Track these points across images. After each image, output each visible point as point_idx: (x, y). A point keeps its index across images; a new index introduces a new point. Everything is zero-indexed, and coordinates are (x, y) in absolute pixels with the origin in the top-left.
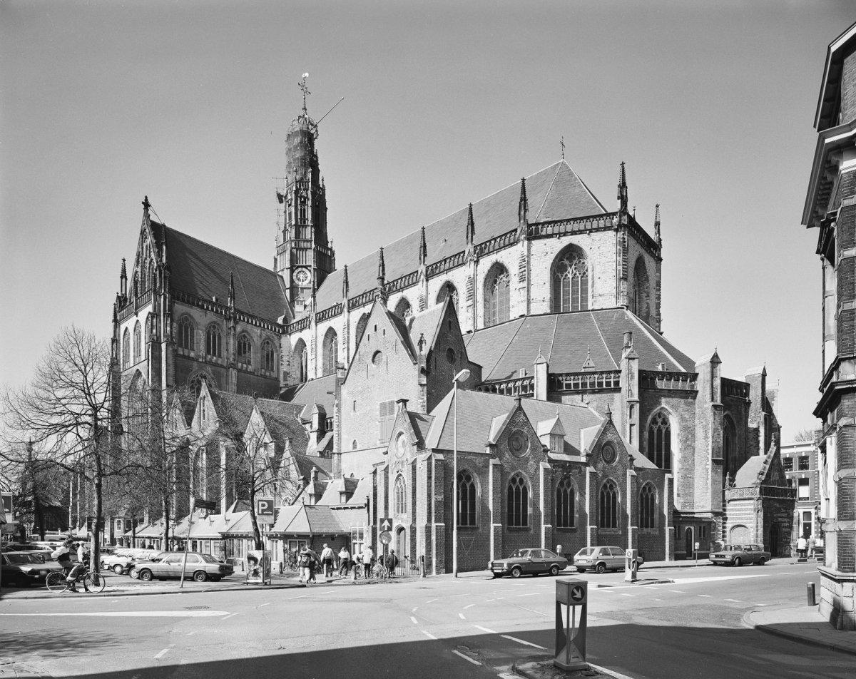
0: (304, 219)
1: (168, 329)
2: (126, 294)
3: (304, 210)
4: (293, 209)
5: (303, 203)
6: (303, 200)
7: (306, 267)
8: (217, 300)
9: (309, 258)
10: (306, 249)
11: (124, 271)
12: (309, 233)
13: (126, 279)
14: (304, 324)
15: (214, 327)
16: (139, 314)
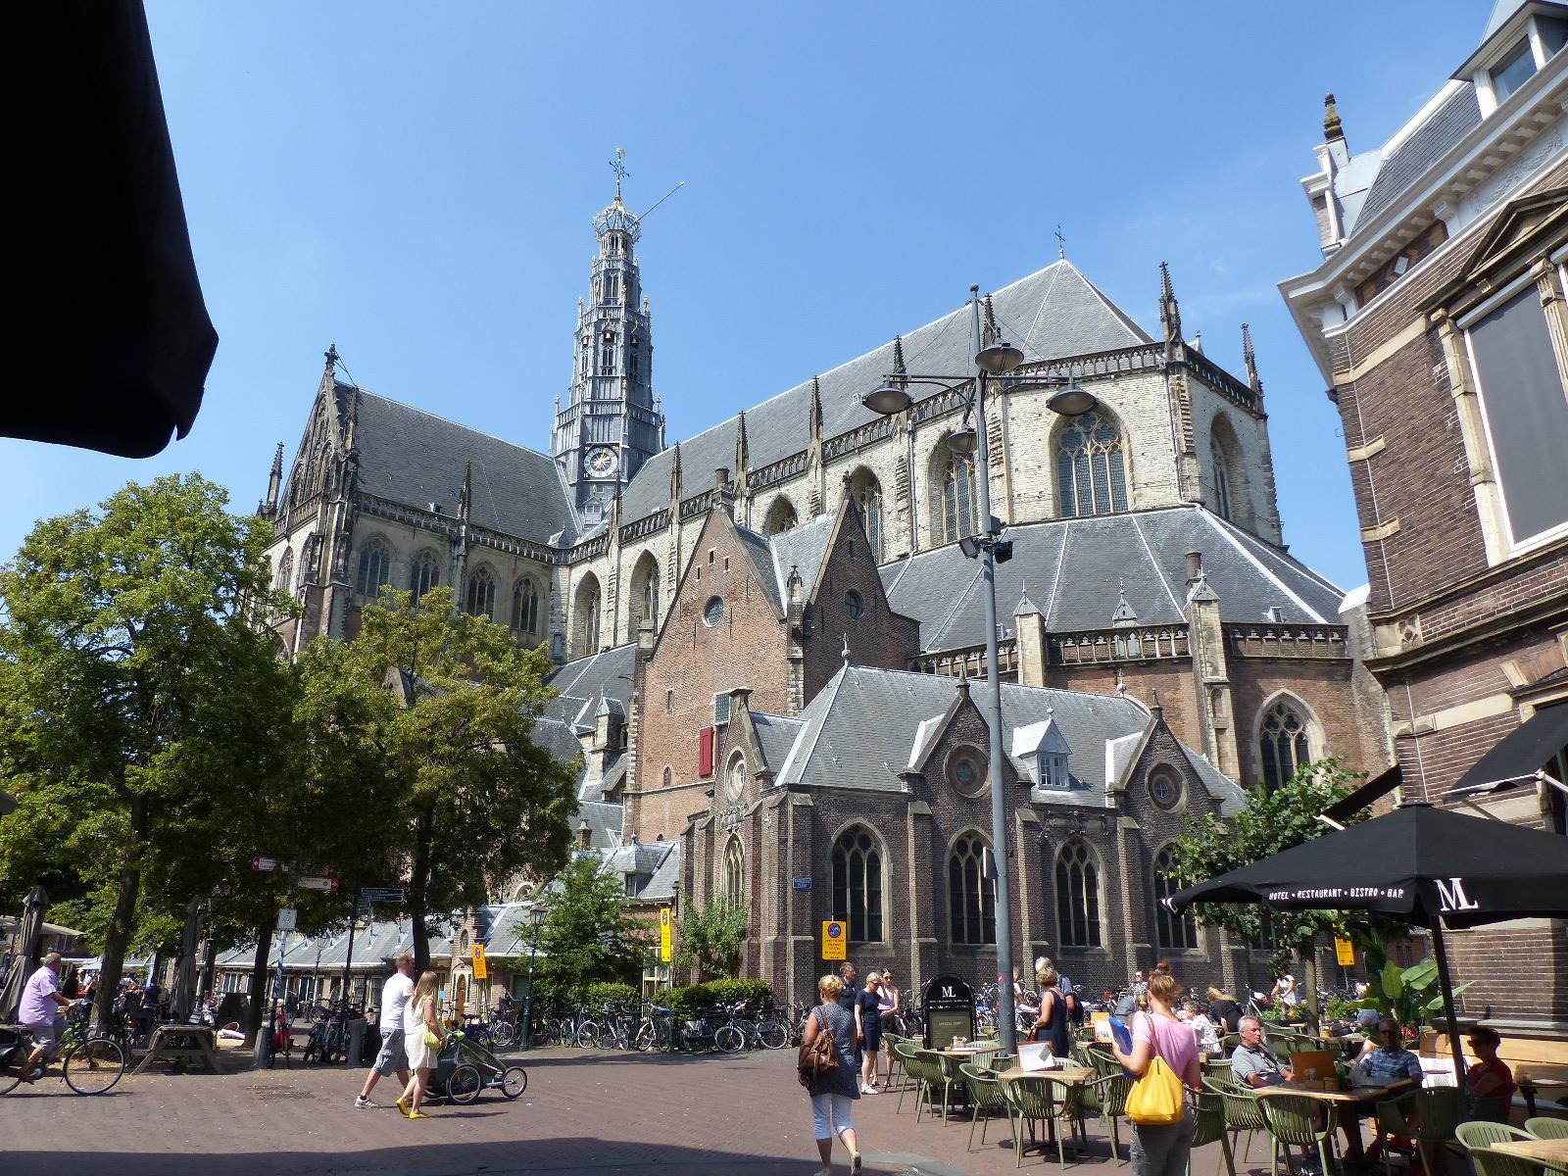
0: (608, 368)
1: (341, 561)
2: (275, 502)
3: (611, 352)
4: (591, 351)
5: (609, 342)
6: (608, 336)
7: (609, 446)
8: (438, 508)
9: (618, 432)
10: (610, 417)
11: (278, 462)
12: (617, 390)
13: (280, 477)
14: (597, 548)
15: (427, 555)
16: (293, 537)
